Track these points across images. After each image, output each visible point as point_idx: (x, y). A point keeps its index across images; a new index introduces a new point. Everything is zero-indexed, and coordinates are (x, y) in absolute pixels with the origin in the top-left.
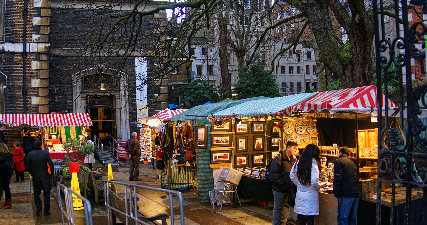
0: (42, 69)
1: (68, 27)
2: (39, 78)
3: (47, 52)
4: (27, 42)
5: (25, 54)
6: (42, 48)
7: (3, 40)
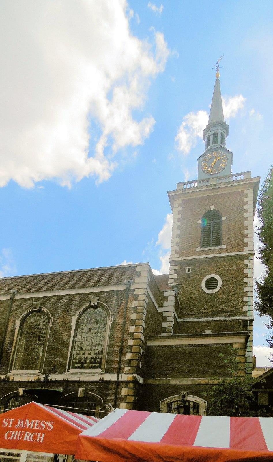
0: (128, 395)
1: (161, 361)
2: (126, 403)
3: (135, 381)
4: (120, 373)
6: (131, 378)
7: (104, 372)
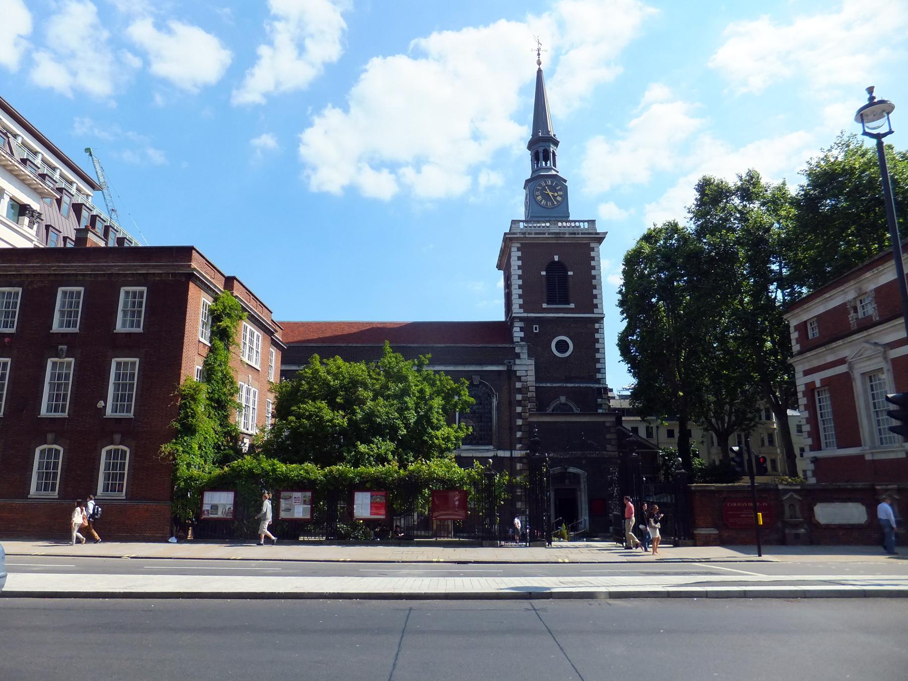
5: (511, 458)
